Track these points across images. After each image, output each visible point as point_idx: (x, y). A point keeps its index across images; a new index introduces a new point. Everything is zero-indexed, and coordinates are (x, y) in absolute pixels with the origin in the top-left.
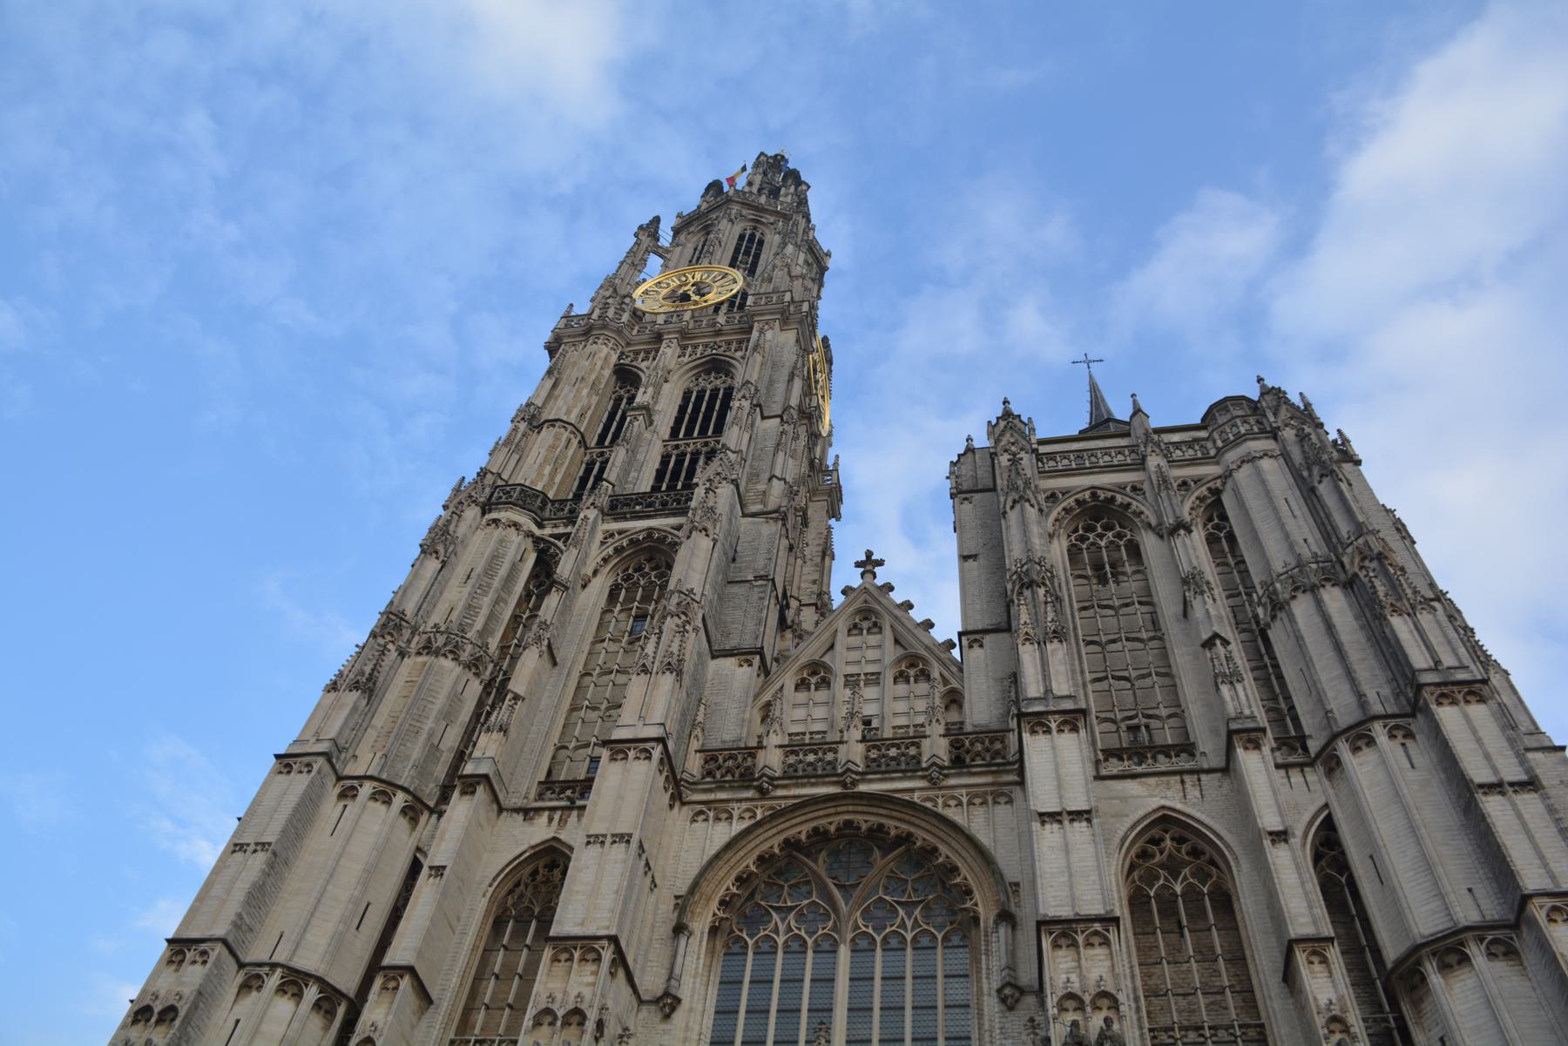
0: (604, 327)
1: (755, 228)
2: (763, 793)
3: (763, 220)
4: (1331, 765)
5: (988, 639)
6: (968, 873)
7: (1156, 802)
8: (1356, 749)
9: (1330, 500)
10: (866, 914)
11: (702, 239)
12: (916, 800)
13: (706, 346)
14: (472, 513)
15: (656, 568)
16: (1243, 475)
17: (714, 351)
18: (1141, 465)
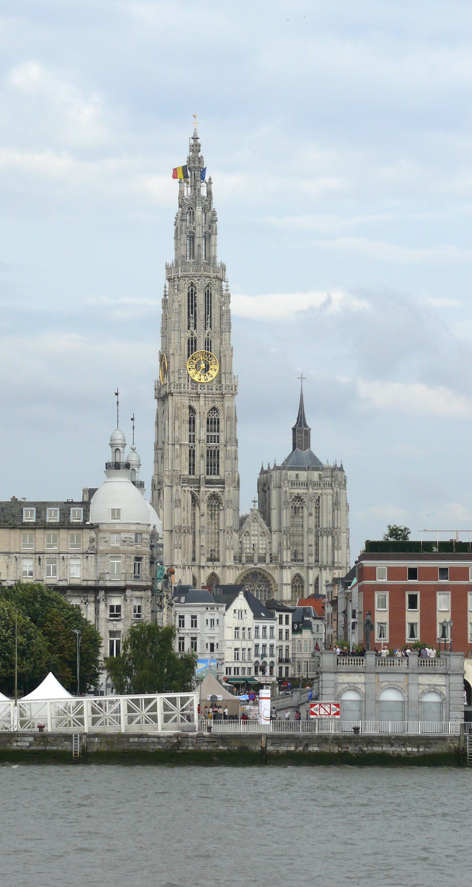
0: (185, 393)
1: (208, 286)
2: (243, 565)
3: (212, 282)
4: (321, 570)
5: (276, 533)
6: (271, 582)
7: (297, 572)
8: (324, 570)
9: (336, 516)
10: (258, 586)
11: (190, 289)
12: (265, 569)
13: (211, 397)
14: (179, 488)
15: (215, 499)
16: (325, 497)
17: (214, 404)
18: (308, 489)
